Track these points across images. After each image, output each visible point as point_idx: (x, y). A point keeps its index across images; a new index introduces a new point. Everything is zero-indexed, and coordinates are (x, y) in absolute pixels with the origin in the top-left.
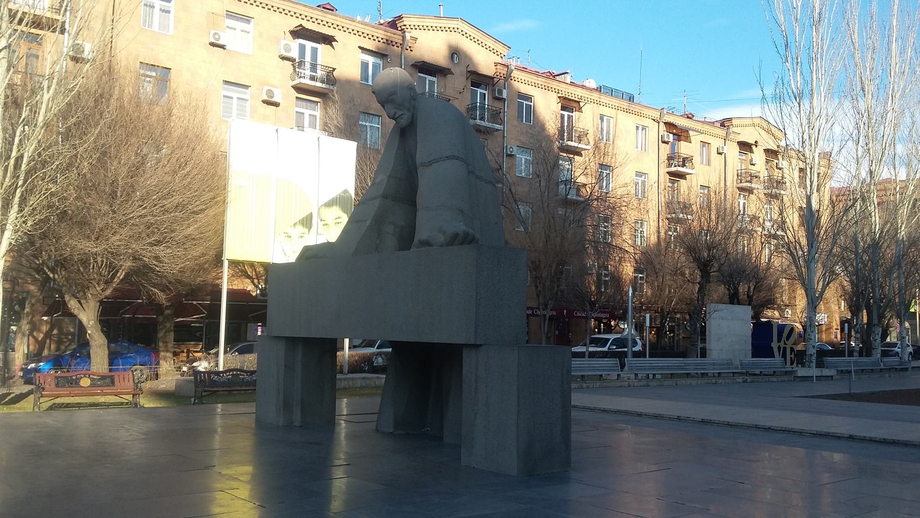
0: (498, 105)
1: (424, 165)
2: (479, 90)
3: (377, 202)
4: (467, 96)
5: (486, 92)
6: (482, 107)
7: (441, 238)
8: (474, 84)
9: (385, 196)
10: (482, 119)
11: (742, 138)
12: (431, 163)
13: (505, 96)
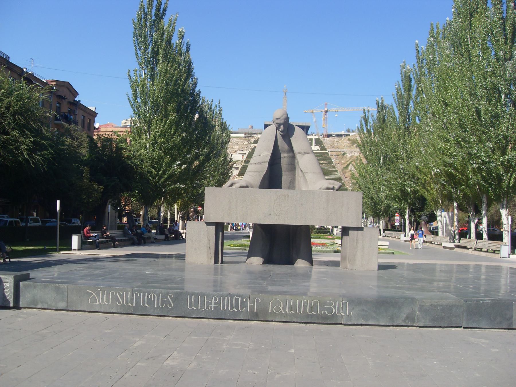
1: (299, 153)
3: (267, 165)
7: (336, 187)
12: (305, 153)
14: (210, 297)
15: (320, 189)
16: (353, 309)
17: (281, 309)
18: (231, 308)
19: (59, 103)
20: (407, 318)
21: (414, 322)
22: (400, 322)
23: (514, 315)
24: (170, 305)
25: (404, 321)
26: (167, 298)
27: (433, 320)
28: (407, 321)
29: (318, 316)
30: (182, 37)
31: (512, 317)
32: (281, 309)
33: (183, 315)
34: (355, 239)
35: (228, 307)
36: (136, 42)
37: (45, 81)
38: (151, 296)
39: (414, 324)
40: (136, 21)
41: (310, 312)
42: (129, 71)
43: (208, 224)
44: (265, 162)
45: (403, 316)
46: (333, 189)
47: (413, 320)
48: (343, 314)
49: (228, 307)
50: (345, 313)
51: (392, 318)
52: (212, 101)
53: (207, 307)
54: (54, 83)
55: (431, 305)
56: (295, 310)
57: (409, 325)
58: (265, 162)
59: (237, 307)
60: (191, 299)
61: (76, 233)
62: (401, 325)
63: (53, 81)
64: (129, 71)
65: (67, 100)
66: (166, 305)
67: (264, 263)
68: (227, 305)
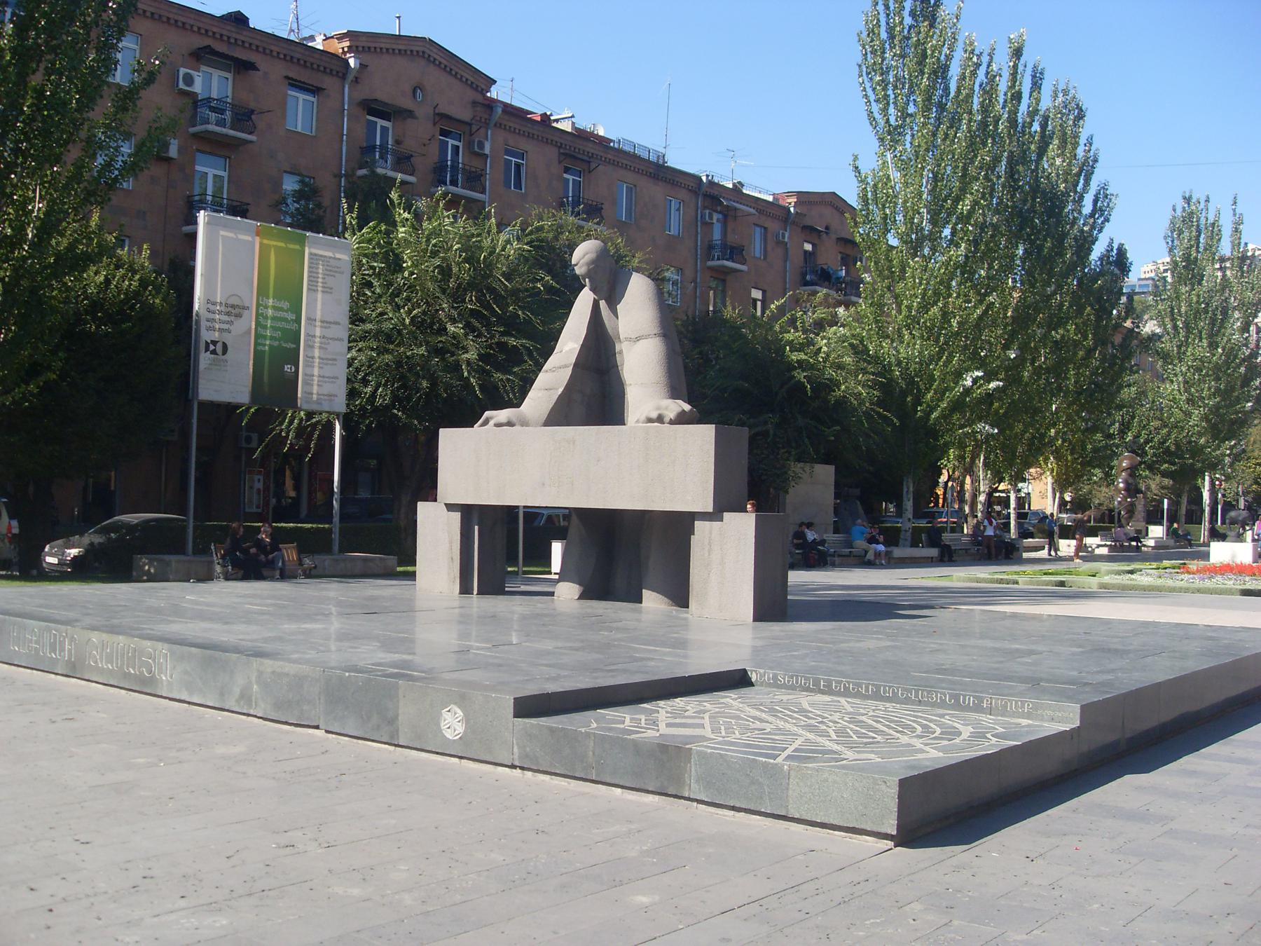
0: (476, 163)
2: (451, 142)
3: (569, 371)
4: (434, 150)
5: (460, 144)
6: (455, 167)
7: (671, 415)
8: (444, 133)
9: (576, 365)
10: (454, 183)
11: (808, 222)
12: (638, 339)
13: (487, 150)
15: (637, 421)
19: (814, 245)
20: (242, 696)
27: (278, 706)
30: (1017, 53)
34: (706, 542)
36: (868, 85)
37: (770, 199)
39: (252, 712)
40: (864, 35)
42: (856, 158)
43: (450, 507)
44: (566, 366)
45: (237, 691)
46: (660, 419)
51: (222, 694)
52: (1207, 201)
54: (793, 200)
55: (273, 672)
58: (566, 366)
61: (557, 538)
63: (790, 194)
64: (856, 158)
65: (834, 237)
67: (583, 596)
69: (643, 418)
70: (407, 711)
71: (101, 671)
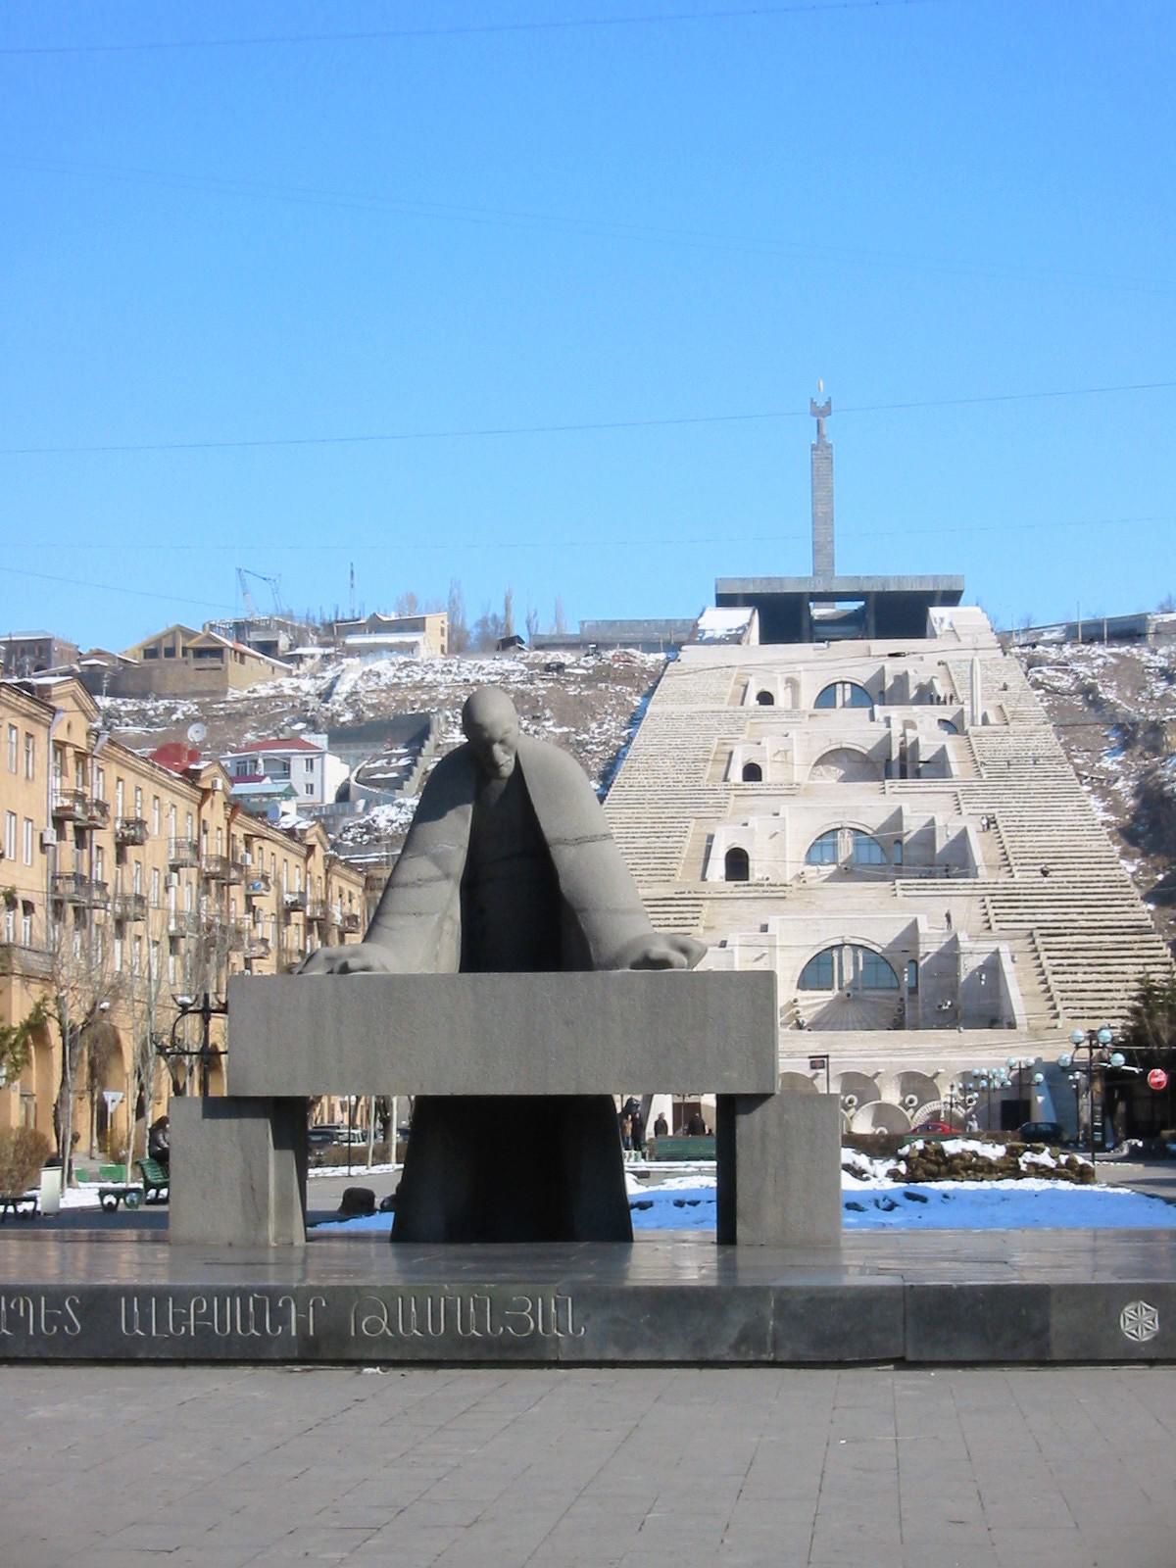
14: (181, 1296)
16: (587, 1318)
17: (384, 1325)
18: (245, 1328)
20: (743, 1338)
21: (762, 1351)
22: (723, 1352)
23: (1053, 1320)
24: (72, 1327)
25: (735, 1347)
26: (62, 1307)
28: (743, 1348)
29: (487, 1342)
31: (1046, 1328)
32: (384, 1325)
33: (110, 1353)
35: (233, 1327)
38: (17, 1305)
39: (764, 1357)
41: (466, 1329)
45: (732, 1333)
47: (760, 1345)
48: (560, 1335)
49: (233, 1327)
50: (564, 1331)
53: (177, 1328)
55: (811, 1300)
56: (422, 1328)
57: (751, 1358)
59: (260, 1326)
60: (130, 1309)
62: (727, 1358)
66: (61, 1329)
68: (232, 1321)
69: (636, 956)
70: (1060, 1320)
71: (399, 1341)
